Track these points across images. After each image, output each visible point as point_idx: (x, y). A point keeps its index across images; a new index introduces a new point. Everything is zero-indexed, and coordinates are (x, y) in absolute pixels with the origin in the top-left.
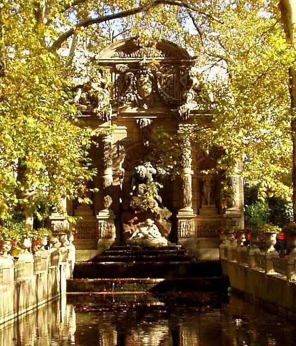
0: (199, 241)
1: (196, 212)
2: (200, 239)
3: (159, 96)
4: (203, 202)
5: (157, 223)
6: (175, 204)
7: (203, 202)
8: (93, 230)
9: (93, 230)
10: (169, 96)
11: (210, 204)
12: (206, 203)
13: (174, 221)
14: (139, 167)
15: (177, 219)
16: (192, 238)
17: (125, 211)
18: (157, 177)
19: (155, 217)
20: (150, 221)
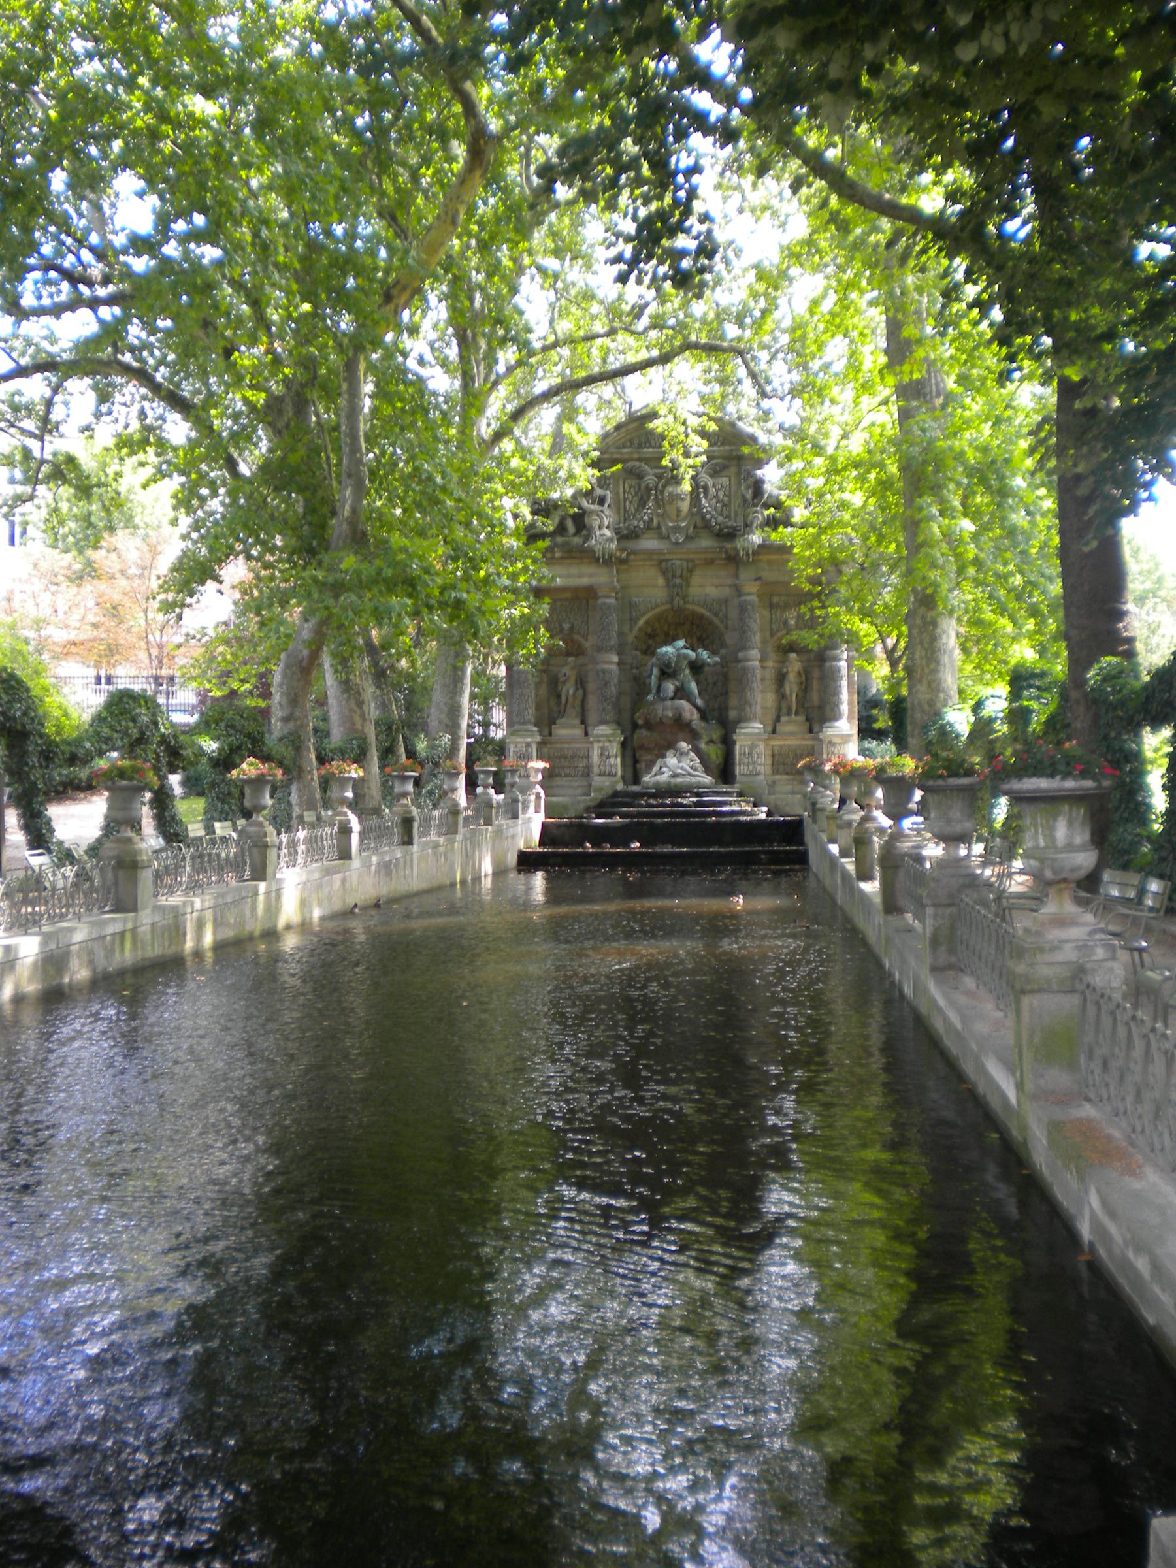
0: (774, 782)
1: (770, 729)
2: (778, 777)
3: (703, 518)
4: (784, 710)
5: (697, 750)
6: (732, 714)
7: (784, 710)
8: (585, 762)
9: (585, 762)
10: (720, 519)
11: (797, 714)
12: (789, 713)
13: (727, 743)
14: (664, 649)
15: (734, 743)
16: (761, 777)
17: (641, 727)
18: (696, 668)
19: (693, 736)
20: (684, 745)
